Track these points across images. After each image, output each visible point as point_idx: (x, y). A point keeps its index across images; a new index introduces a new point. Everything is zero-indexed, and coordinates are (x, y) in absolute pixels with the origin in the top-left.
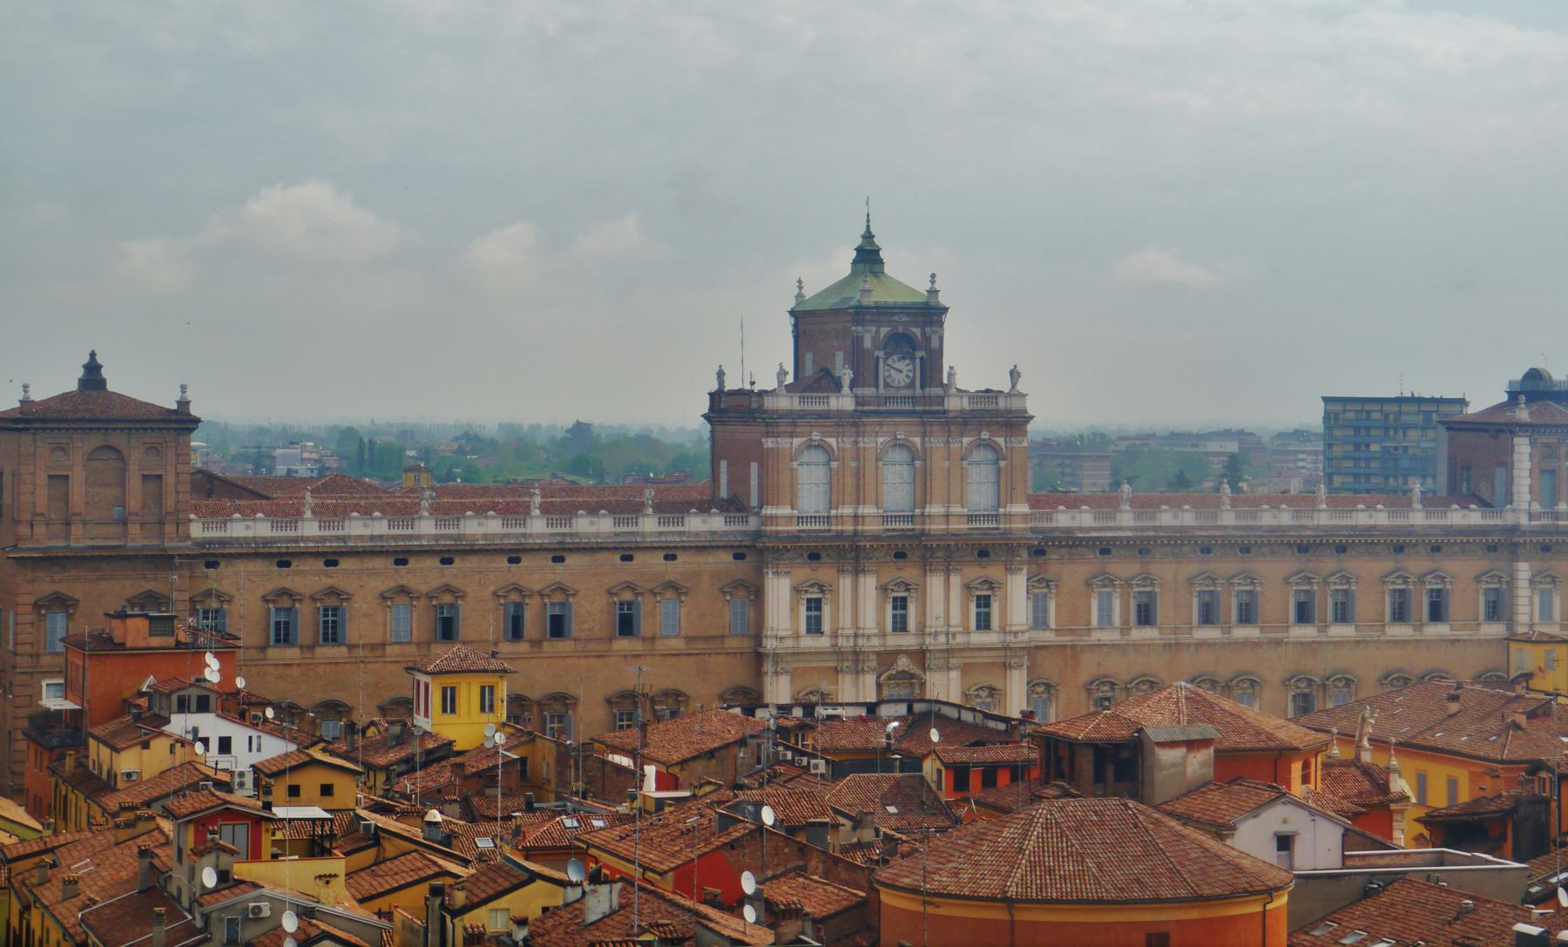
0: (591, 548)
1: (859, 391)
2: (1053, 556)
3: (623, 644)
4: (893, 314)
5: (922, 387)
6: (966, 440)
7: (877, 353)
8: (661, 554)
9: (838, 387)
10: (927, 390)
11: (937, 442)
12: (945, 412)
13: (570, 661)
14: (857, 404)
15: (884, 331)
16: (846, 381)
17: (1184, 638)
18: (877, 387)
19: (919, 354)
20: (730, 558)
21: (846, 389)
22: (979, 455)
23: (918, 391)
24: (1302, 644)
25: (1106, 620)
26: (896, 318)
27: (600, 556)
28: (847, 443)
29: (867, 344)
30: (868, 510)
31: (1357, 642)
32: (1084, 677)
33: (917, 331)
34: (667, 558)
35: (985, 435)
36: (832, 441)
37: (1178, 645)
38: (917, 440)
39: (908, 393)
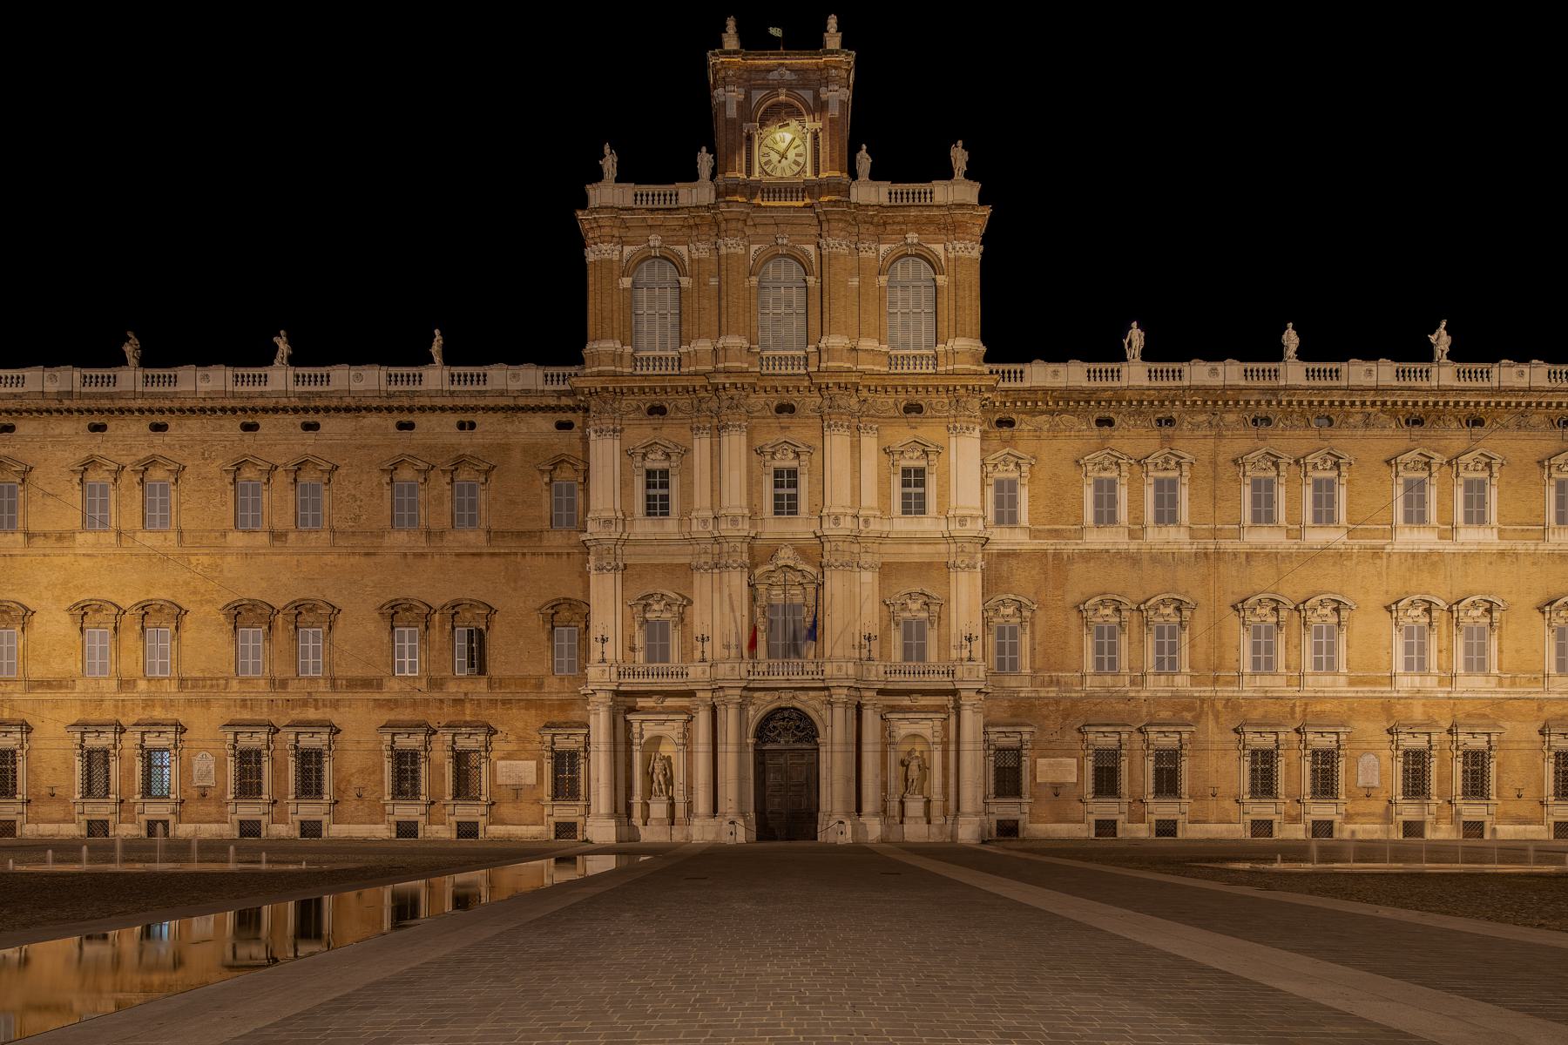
0: (355, 409)
2: (1025, 425)
3: (400, 539)
5: (817, 173)
6: (883, 248)
8: (453, 419)
11: (837, 244)
13: (328, 559)
17: (1228, 545)
20: (552, 427)
22: (908, 271)
23: (809, 175)
24: (1414, 555)
25: (1106, 515)
27: (372, 420)
28: (702, 251)
30: (734, 341)
31: (1502, 554)
32: (1073, 597)
34: (461, 426)
35: (912, 237)
36: (683, 249)
37: (1219, 554)
38: (811, 249)
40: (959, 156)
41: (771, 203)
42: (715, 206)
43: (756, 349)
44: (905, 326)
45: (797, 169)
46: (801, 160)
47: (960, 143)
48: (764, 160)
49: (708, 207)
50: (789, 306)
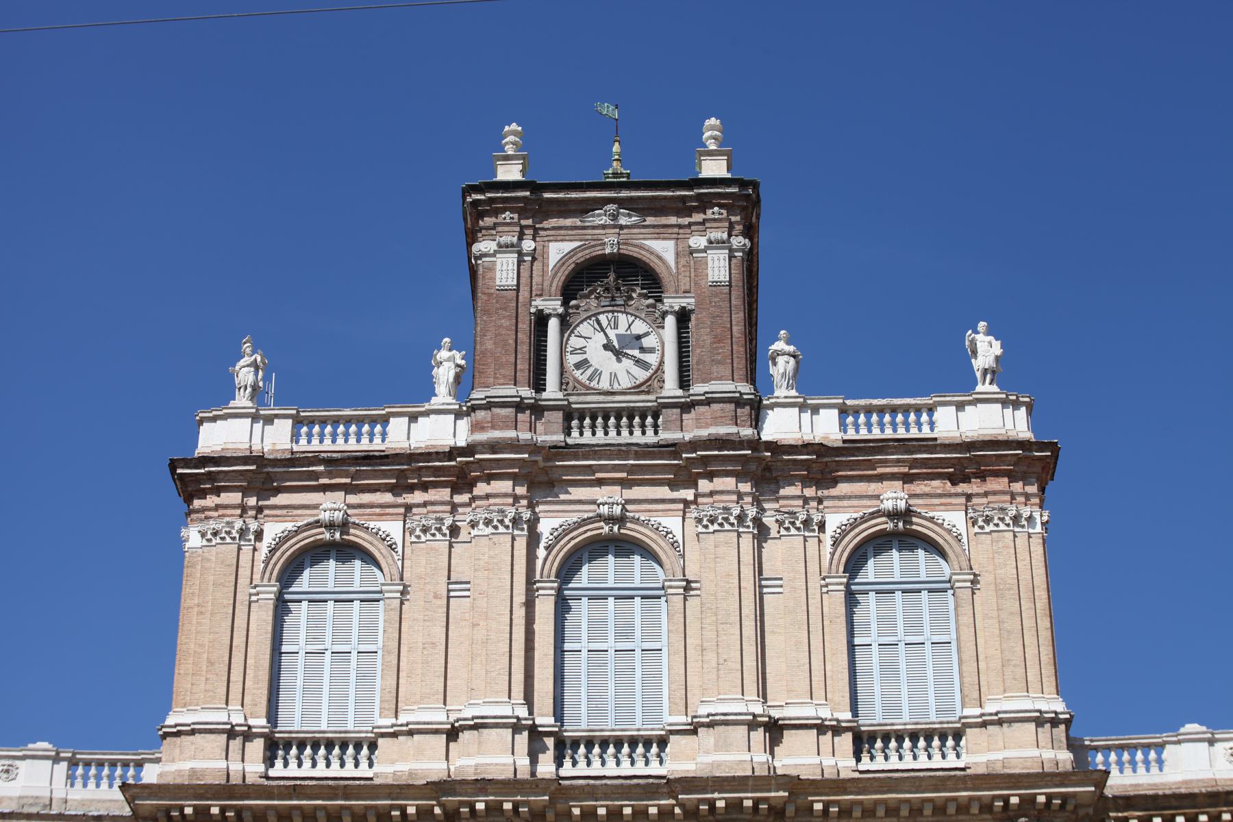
1: (478, 395)
4: (585, 208)
5: (684, 383)
7: (539, 303)
9: (414, 393)
10: (698, 389)
12: (756, 444)
14: (476, 427)
15: (557, 251)
16: (444, 374)
18: (538, 384)
19: (673, 302)
21: (443, 396)
23: (671, 388)
26: (599, 218)
29: (504, 271)
33: (662, 250)
35: (893, 496)
36: (394, 528)
39: (640, 401)
40: (987, 349)
41: (588, 438)
42: (470, 450)
43: (545, 720)
44: (890, 670)
45: (642, 375)
46: (652, 359)
47: (982, 325)
48: (572, 360)
49: (453, 452)
50: (624, 632)
